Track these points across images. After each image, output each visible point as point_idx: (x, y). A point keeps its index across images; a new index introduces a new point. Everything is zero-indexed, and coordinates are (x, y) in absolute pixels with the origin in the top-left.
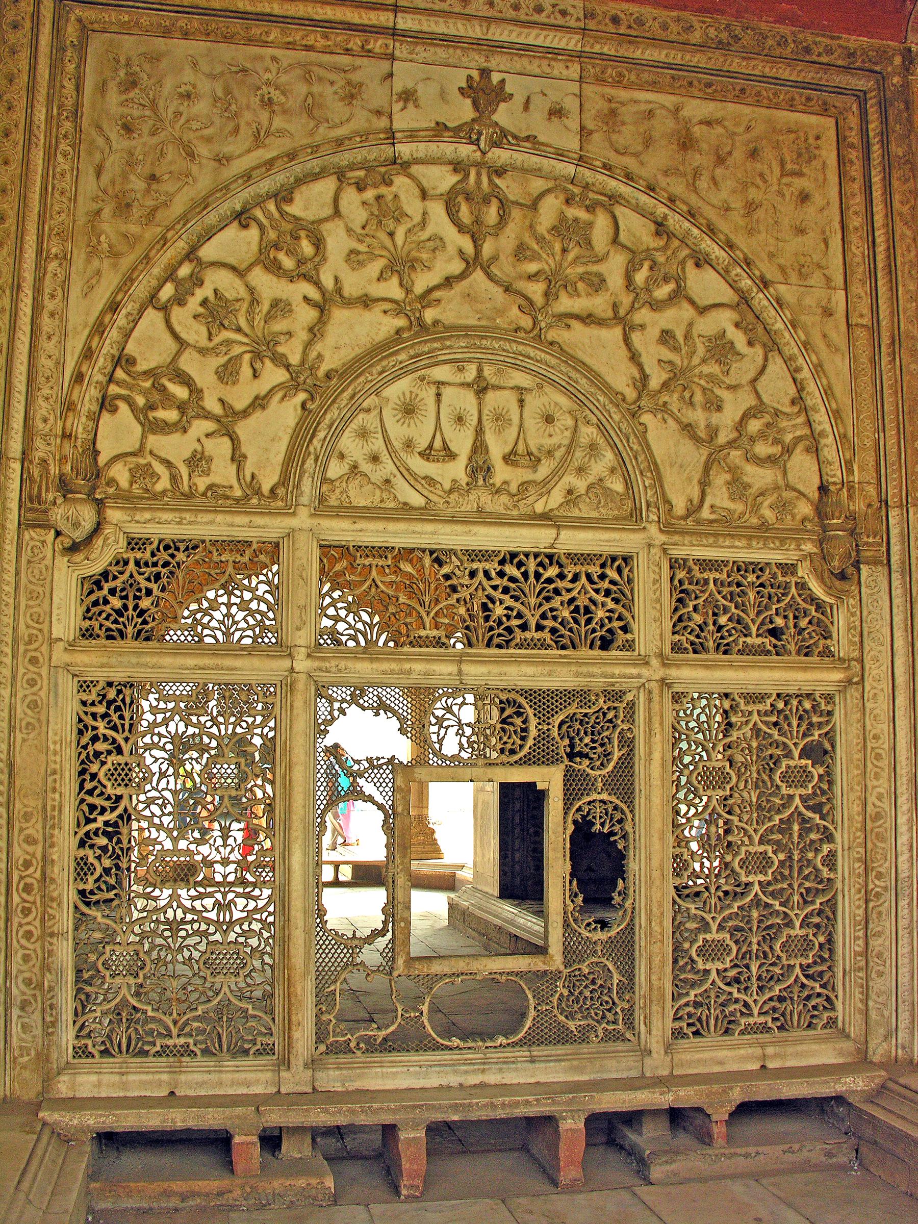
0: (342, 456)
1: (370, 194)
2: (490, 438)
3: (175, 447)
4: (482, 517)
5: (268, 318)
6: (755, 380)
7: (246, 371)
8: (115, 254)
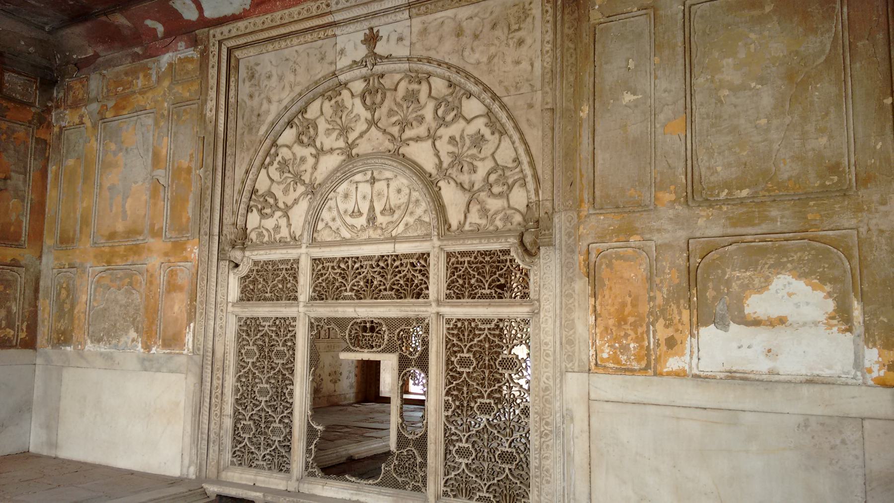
0: (322, 220)
1: (333, 101)
2: (376, 204)
3: (269, 223)
4: (369, 241)
5: (299, 165)
6: (494, 153)
7: (292, 189)
8: (248, 150)
